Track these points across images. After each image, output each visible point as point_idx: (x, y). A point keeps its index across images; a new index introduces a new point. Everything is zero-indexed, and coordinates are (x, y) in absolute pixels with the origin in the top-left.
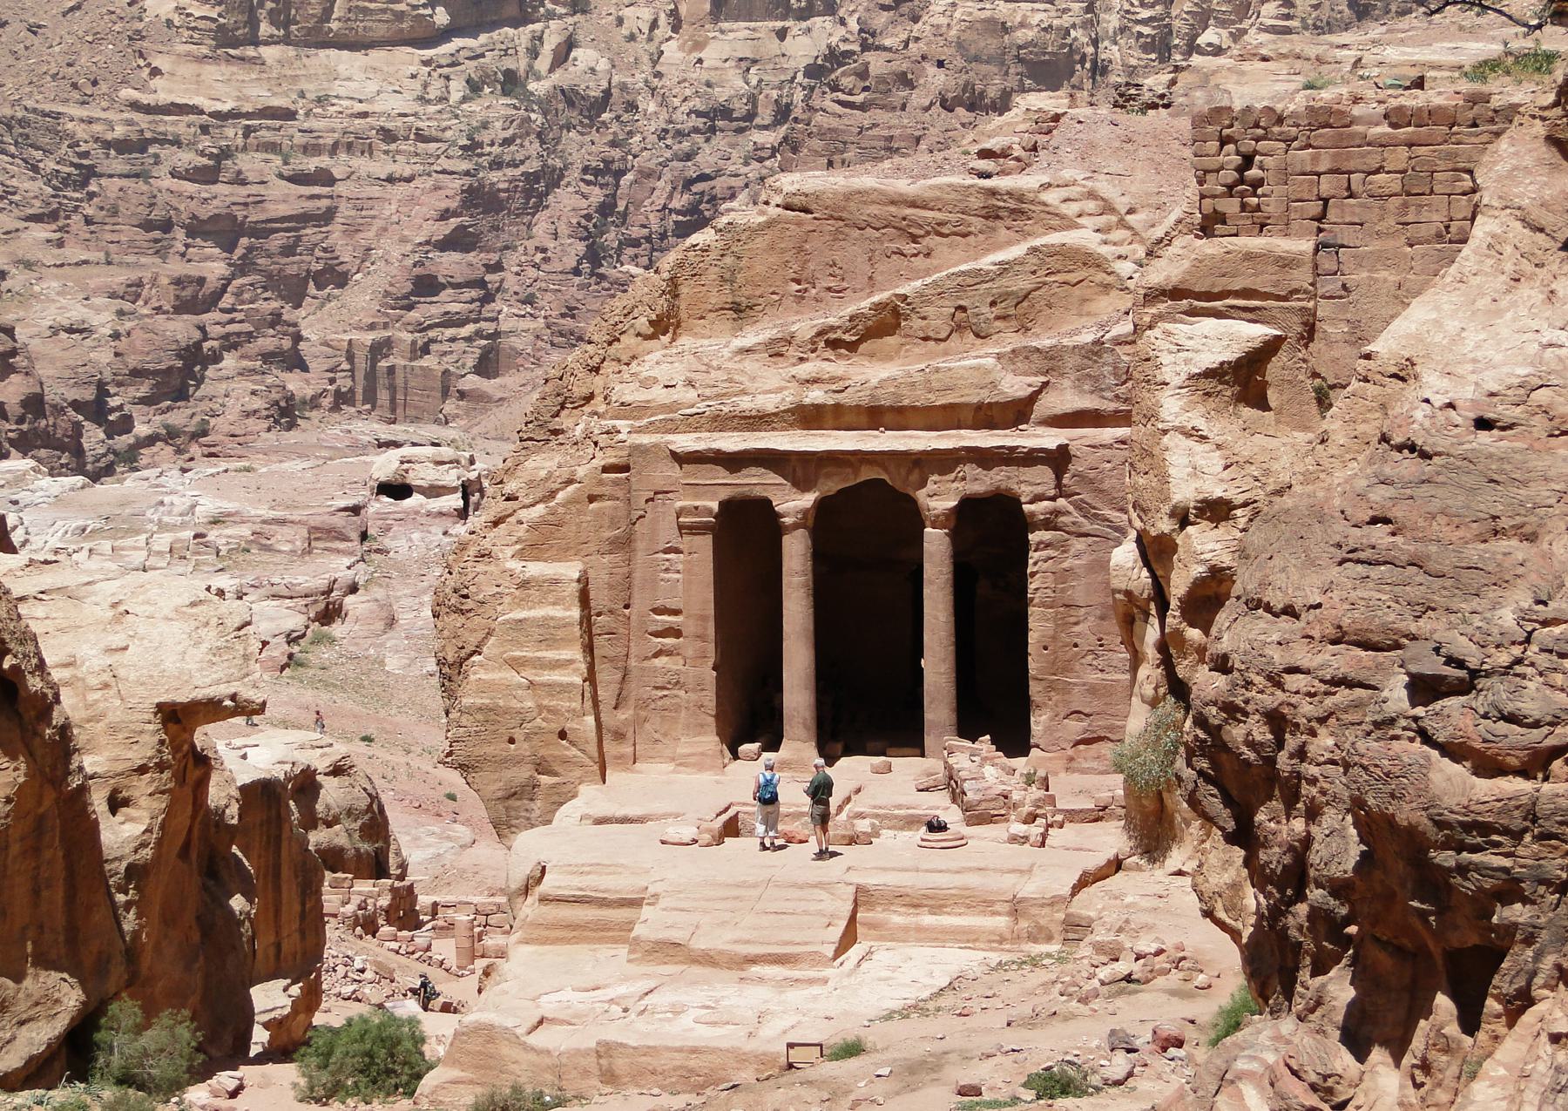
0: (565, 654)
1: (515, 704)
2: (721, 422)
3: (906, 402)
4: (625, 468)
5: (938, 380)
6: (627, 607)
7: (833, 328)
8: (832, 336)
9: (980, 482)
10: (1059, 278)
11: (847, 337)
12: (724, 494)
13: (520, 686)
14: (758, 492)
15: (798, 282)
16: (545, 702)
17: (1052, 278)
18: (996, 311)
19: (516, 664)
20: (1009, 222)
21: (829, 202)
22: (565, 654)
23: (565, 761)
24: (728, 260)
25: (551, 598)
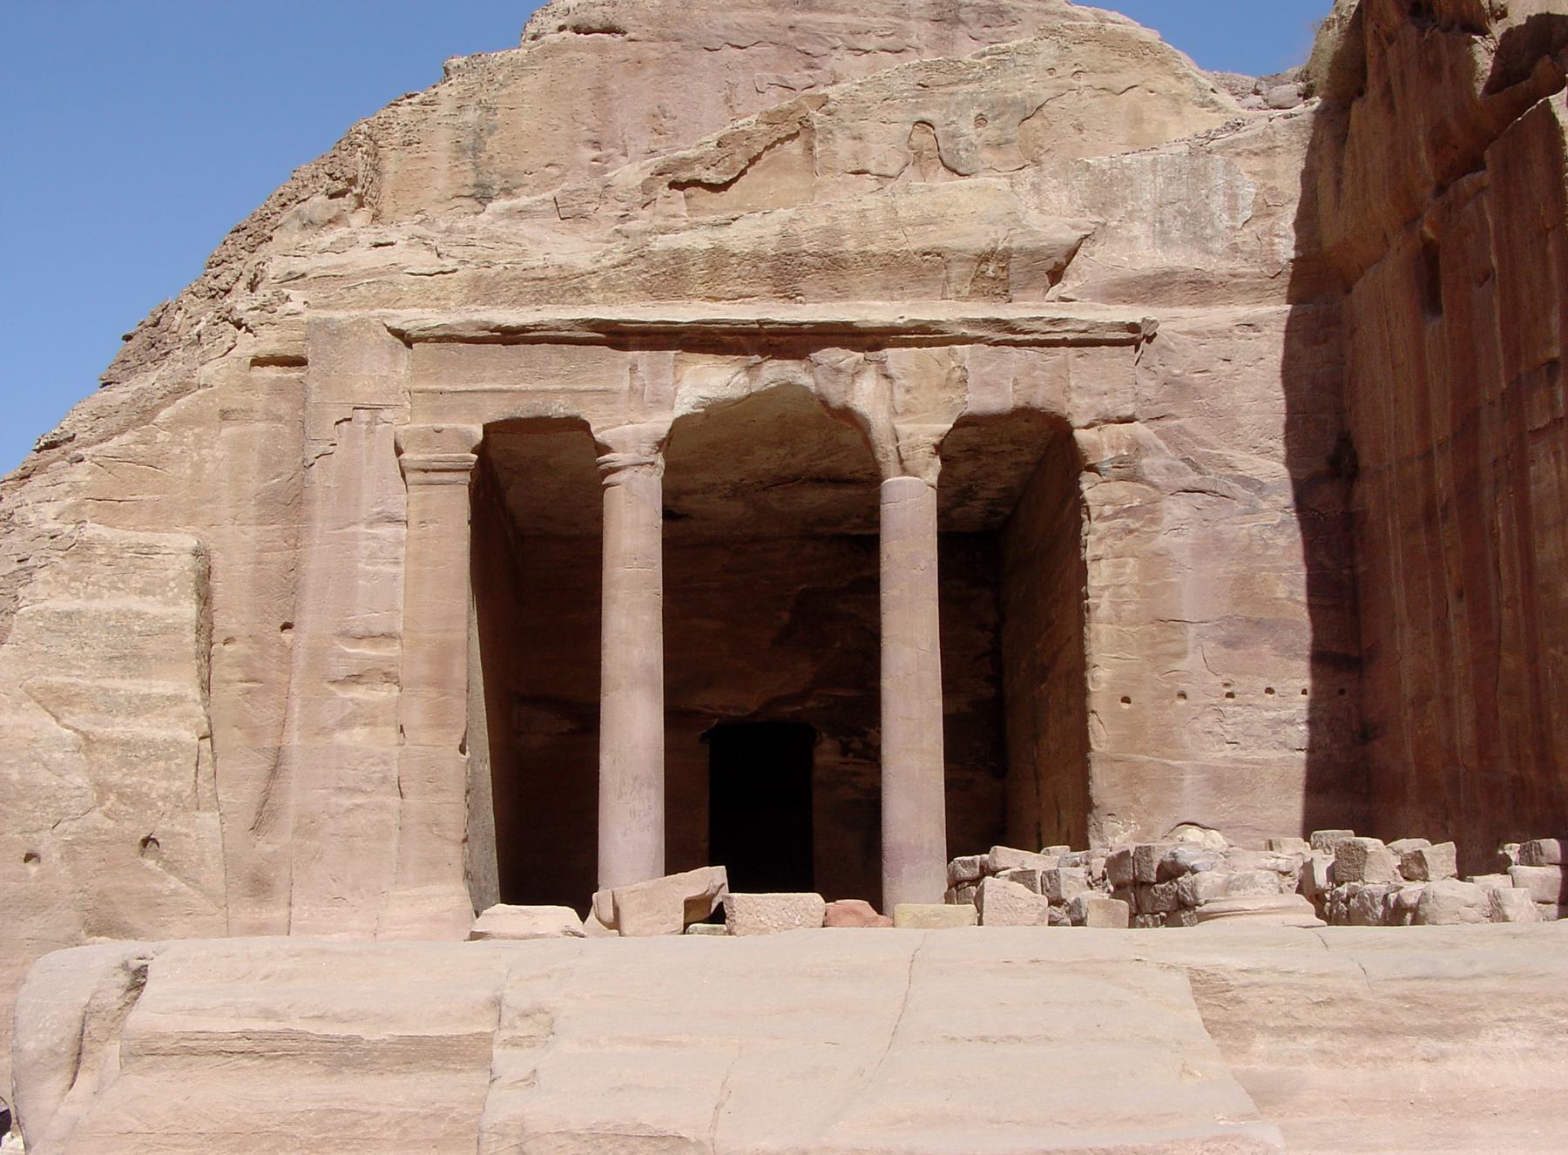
0: (162, 686)
1: (44, 777)
2: (484, 290)
3: (850, 245)
4: (299, 362)
5: (911, 206)
6: (287, 626)
7: (685, 163)
8: (684, 176)
9: (999, 384)
10: (1098, 80)
11: (711, 176)
12: (496, 411)
13: (60, 742)
14: (560, 408)
15: (596, 144)
16: (115, 777)
17: (1083, 81)
18: (990, 132)
19: (57, 701)
20: (977, 30)
21: (655, 13)
22: (162, 686)
23: (151, 903)
24: (471, 116)
25: (137, 581)
